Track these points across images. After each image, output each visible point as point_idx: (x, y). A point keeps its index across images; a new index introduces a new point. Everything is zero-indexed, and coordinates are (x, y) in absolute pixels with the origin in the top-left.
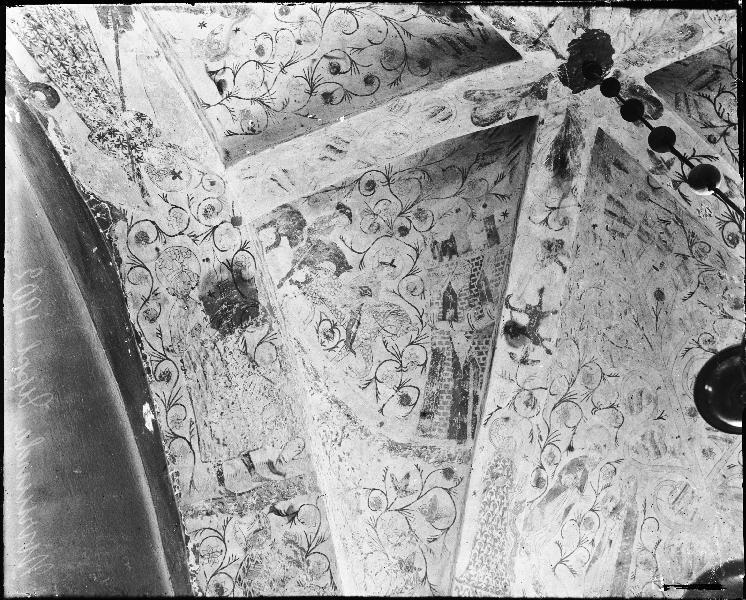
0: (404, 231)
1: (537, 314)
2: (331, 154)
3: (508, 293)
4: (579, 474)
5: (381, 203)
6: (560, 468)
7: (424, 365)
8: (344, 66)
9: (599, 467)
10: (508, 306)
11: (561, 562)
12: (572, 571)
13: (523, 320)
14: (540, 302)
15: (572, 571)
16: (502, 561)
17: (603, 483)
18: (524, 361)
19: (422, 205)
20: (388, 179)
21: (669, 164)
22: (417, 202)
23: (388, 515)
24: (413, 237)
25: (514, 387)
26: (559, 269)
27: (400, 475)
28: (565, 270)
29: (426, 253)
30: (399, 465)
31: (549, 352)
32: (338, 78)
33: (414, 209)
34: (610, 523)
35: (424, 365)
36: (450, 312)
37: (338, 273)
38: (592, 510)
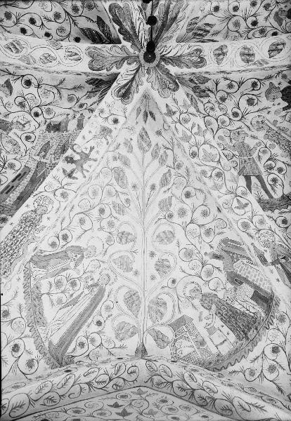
0: (37, 115)
1: (86, 157)
4: (79, 256)
6: (69, 245)
7: (17, 171)
8: (39, 23)
9: (91, 259)
10: (73, 149)
11: (48, 294)
13: (77, 157)
15: (52, 302)
16: (10, 260)
17: (89, 269)
18: (70, 176)
19: (50, 107)
20: (39, 85)
21: (174, 113)
22: (49, 104)
24: (40, 119)
26: (105, 142)
29: (44, 127)
31: (85, 177)
33: (46, 107)
34: (86, 291)
36: (43, 153)
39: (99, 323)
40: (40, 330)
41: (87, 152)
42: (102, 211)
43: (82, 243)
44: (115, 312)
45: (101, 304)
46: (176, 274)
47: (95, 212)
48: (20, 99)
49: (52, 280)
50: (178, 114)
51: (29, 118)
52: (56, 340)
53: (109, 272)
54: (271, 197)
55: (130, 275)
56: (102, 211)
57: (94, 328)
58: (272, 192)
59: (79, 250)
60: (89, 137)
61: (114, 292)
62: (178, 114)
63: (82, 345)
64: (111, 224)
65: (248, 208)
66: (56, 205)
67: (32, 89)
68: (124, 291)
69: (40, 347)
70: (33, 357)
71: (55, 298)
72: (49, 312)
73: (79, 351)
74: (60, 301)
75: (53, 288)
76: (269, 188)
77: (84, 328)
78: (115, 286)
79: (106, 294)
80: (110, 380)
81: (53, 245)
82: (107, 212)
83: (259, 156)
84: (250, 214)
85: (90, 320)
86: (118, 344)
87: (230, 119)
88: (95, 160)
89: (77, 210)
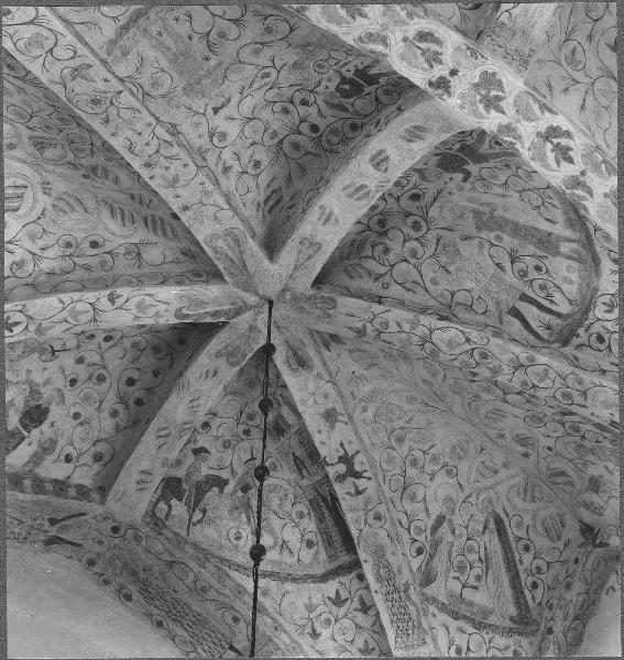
0: (247, 432)
2: (162, 440)
3: (322, 456)
5: (221, 428)
6: (429, 532)
8: (136, 375)
11: (464, 586)
12: (474, 587)
14: (346, 452)
15: (474, 587)
18: (359, 493)
23: (338, 625)
25: (361, 513)
27: (333, 595)
28: (346, 423)
30: (331, 587)
31: (370, 479)
32: (137, 385)
33: (244, 416)
34: (486, 538)
35: (309, 514)
37: (221, 491)
38: (468, 539)
39: (527, 548)
40: (492, 619)
41: (342, 453)
42: (414, 463)
43: (436, 509)
44: (527, 520)
45: (509, 531)
46: (545, 442)
47: (412, 472)
48: (220, 442)
49: (452, 574)
50: (368, 325)
51: (246, 444)
52: (512, 610)
53: (483, 496)
54: (559, 315)
55: (503, 473)
56: (414, 463)
57: (527, 558)
58: (554, 308)
59: (440, 520)
60: (323, 437)
61: (507, 505)
62: (368, 325)
63: (535, 585)
64: (435, 459)
65: (552, 375)
66: (383, 534)
67: (215, 423)
68: (513, 493)
69: (510, 632)
70: (513, 648)
71: (472, 581)
72: (480, 598)
73: (539, 593)
74: (478, 578)
75: (461, 578)
76: (546, 303)
77: (521, 568)
78: (503, 498)
79: (502, 515)
80: (587, 593)
81: (419, 551)
82: (418, 454)
83: (497, 264)
84: (558, 380)
85: (517, 558)
86: (560, 545)
87: (417, 239)
88: (358, 452)
89: (396, 496)
